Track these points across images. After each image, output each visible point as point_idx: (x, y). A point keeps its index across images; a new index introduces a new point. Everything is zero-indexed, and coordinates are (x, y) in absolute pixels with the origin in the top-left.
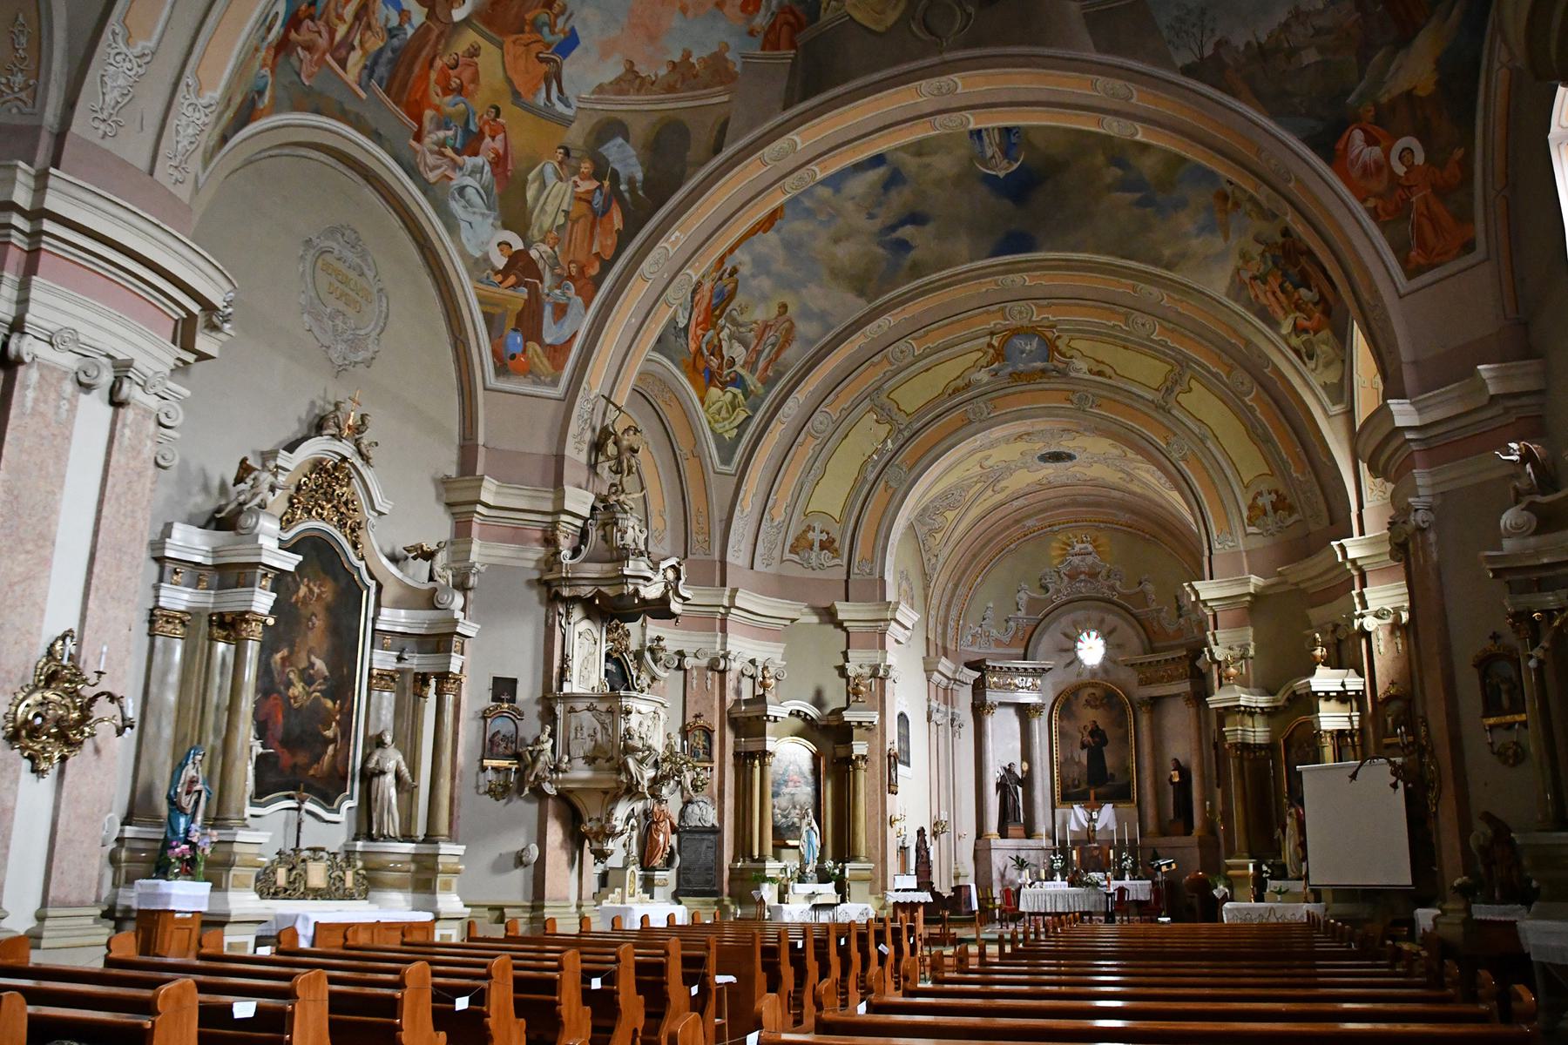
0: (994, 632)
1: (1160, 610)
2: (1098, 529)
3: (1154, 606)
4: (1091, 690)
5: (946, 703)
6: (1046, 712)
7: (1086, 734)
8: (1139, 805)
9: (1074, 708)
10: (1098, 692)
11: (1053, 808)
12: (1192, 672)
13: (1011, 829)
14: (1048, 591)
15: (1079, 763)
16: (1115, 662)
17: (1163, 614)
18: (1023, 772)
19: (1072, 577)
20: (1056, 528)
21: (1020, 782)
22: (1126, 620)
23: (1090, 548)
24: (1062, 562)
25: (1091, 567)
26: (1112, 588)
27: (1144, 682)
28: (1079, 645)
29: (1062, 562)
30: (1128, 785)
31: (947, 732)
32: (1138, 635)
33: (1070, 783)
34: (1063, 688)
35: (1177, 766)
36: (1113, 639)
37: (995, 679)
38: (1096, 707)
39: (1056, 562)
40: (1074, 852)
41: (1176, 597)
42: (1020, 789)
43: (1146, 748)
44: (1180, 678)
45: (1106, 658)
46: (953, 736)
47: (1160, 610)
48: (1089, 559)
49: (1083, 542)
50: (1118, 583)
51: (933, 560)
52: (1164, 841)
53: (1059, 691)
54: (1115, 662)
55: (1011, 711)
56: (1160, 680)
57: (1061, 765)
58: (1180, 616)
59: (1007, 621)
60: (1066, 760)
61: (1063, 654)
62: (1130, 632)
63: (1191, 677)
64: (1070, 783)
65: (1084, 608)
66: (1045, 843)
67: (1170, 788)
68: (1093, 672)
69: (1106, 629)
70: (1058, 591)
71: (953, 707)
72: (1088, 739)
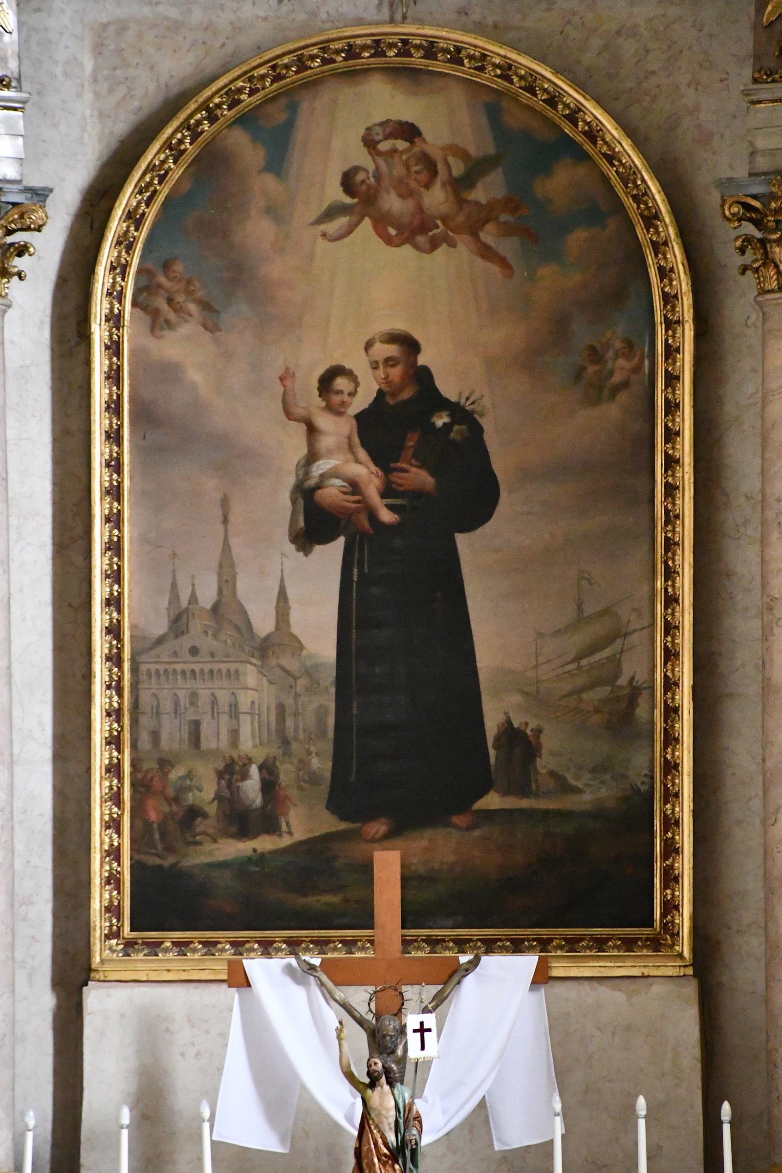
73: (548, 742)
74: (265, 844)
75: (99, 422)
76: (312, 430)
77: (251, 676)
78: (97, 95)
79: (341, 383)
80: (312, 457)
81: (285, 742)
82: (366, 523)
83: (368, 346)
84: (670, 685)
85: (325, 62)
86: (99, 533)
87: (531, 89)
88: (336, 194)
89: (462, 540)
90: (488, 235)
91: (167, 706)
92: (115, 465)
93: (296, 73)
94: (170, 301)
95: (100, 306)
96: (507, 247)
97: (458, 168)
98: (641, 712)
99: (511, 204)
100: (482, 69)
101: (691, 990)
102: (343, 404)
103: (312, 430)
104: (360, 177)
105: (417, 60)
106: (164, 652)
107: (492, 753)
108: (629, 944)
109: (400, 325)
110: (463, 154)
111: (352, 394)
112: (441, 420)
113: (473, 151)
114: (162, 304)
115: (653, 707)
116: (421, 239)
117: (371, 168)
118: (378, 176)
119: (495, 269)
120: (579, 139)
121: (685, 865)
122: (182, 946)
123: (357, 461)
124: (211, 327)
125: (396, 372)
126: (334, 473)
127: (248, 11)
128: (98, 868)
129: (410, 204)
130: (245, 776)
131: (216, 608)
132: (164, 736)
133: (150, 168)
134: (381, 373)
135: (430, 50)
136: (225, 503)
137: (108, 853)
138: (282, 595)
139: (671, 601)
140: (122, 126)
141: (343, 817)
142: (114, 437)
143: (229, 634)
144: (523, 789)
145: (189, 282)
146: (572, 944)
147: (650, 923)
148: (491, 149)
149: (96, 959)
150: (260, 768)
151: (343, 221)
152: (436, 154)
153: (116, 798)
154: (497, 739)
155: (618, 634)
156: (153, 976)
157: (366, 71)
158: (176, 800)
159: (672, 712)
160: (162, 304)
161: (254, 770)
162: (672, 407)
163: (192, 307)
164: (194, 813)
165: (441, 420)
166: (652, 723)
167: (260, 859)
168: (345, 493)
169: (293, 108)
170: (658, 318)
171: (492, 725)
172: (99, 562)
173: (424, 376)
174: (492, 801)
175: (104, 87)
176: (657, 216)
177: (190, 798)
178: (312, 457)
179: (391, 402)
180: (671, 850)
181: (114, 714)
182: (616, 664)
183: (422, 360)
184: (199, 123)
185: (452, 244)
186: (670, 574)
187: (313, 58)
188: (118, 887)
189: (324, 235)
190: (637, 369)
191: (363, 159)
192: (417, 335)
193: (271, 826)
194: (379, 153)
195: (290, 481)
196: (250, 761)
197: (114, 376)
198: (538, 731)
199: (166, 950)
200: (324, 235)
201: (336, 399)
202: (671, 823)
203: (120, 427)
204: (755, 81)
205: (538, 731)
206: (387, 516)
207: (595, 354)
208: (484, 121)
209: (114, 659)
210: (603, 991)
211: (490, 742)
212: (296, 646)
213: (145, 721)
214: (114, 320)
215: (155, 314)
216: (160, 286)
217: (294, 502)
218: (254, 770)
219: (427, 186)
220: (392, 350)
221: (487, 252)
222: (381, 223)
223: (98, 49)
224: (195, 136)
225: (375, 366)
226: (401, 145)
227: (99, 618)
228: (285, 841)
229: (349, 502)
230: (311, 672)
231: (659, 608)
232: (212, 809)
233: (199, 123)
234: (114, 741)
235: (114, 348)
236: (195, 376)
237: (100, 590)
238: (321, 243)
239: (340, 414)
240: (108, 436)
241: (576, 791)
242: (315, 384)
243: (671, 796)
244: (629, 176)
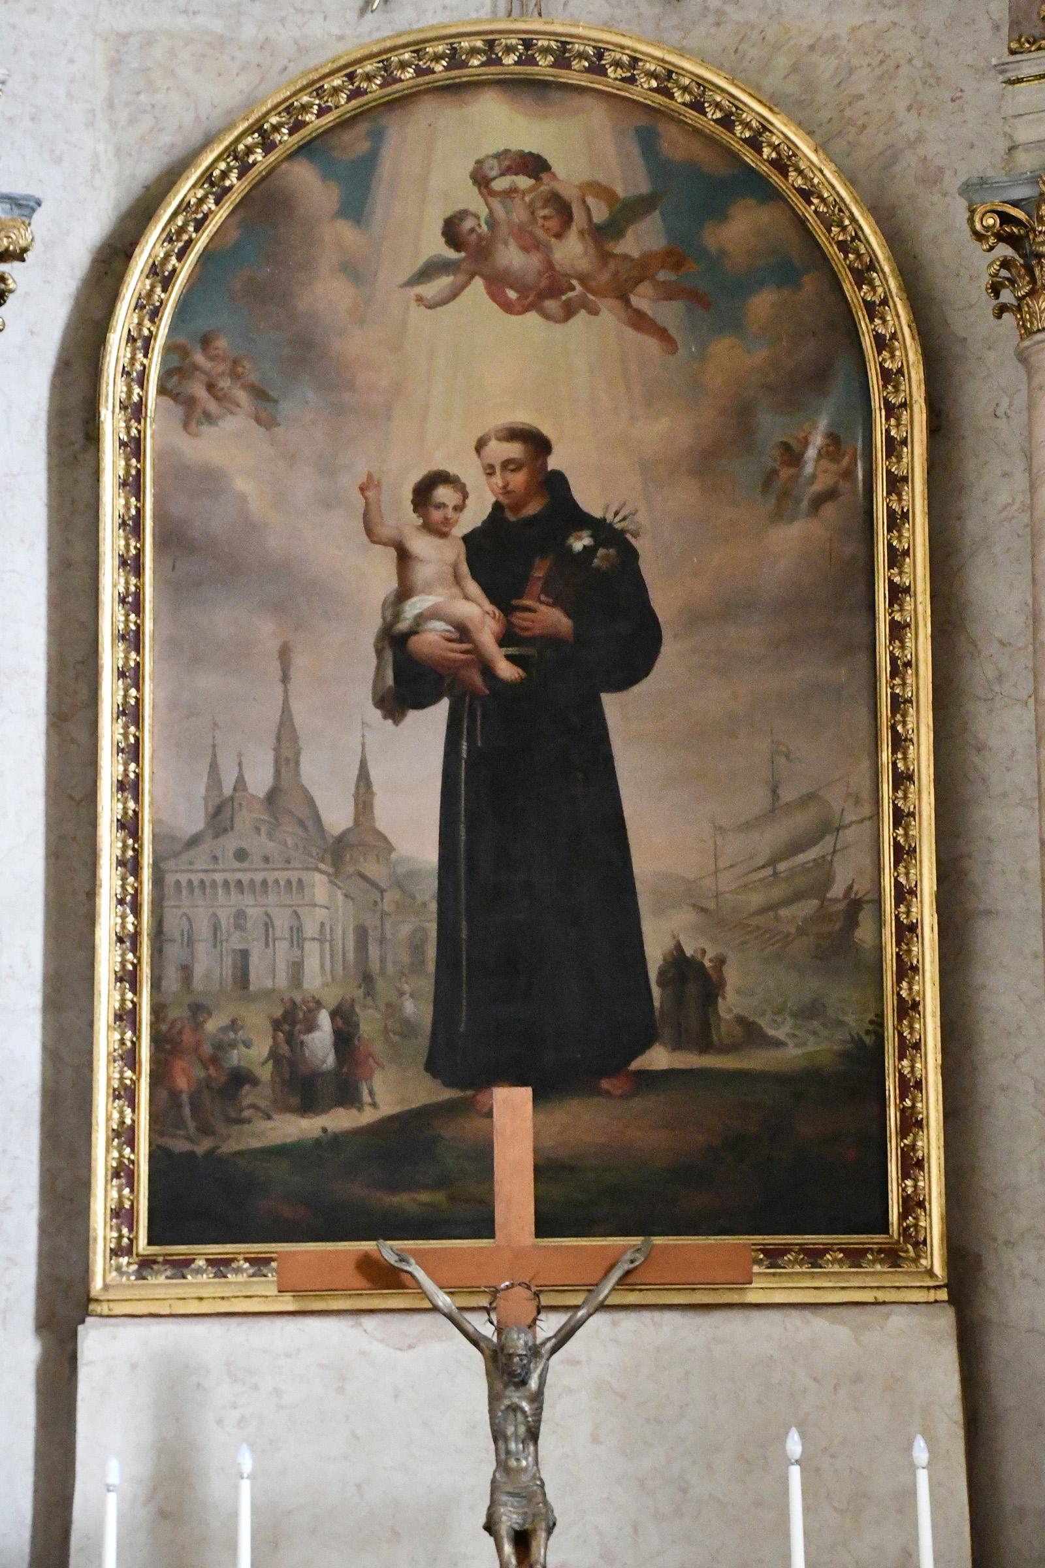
73: (732, 976)
74: (340, 1120)
75: (111, 543)
76: (404, 557)
77: (320, 886)
78: (113, 125)
79: (443, 494)
80: (404, 592)
81: (367, 979)
82: (477, 680)
83: (480, 445)
84: (904, 894)
85: (420, 72)
86: (110, 692)
87: (697, 106)
88: (436, 247)
89: (610, 702)
90: (642, 300)
91: (203, 930)
92: (133, 603)
93: (381, 86)
94: (211, 387)
95: (113, 388)
96: (669, 314)
97: (600, 212)
98: (863, 934)
99: (674, 258)
100: (632, 80)
101: (946, 1321)
102: (446, 521)
103: (404, 557)
104: (468, 224)
106: (200, 857)
107: (656, 991)
108: (855, 1256)
109: (523, 417)
110: (605, 193)
111: (459, 508)
112: (580, 542)
113: (620, 191)
114: (200, 392)
115: (880, 924)
116: (551, 305)
117: (484, 212)
118: (492, 222)
119: (651, 344)
120: (765, 168)
122: (220, 1265)
123: (467, 598)
124: (266, 421)
125: (518, 480)
126: (434, 614)
127: (317, 28)
128: (102, 1157)
130: (311, 1027)
131: (272, 797)
132: (199, 971)
133: (184, 207)
134: (498, 480)
136: (285, 654)
137: (117, 1134)
138: (364, 776)
140: (146, 168)
142: (132, 564)
143: (290, 833)
145: (235, 362)
146: (773, 1256)
147: (884, 1228)
148: (644, 188)
149: (97, 1284)
150: (333, 1015)
151: (444, 282)
152: (570, 193)
153: (130, 1058)
154: (662, 973)
155: (827, 827)
156: (181, 1308)
157: (475, 85)
158: (215, 1060)
159: (907, 931)
160: (200, 392)
161: (324, 1018)
163: (242, 396)
164: (240, 1078)
165: (580, 542)
166: (880, 948)
167: (333, 1142)
168: (449, 640)
169: (377, 137)
170: (876, 402)
171: (655, 952)
172: (109, 731)
173: (556, 485)
174: (658, 1058)
175: (123, 115)
176: (872, 266)
177: (235, 1057)
178: (404, 592)
179: (511, 517)
180: (911, 1123)
181: (128, 940)
182: (825, 867)
183: (553, 463)
184: (249, 150)
185: (594, 312)
186: (899, 743)
187: (403, 65)
188: (131, 1184)
189: (420, 299)
190: (849, 474)
191: (471, 200)
192: (547, 430)
193: (347, 1095)
194: (493, 193)
195: (374, 624)
196: (319, 1004)
197: (133, 485)
198: (720, 961)
199: (199, 1271)
200: (420, 299)
201: (436, 515)
202: (911, 1086)
203: (140, 552)
204: (1013, 52)
205: (720, 961)
206: (506, 670)
207: (792, 455)
208: (635, 150)
209: (130, 865)
210: (818, 1323)
211: (653, 975)
212: (384, 846)
213: (174, 952)
215: (189, 403)
216: (196, 367)
217: (379, 652)
218: (324, 1019)
219: (559, 236)
220: (514, 450)
221: (639, 321)
222: (497, 284)
223: (115, 64)
225: (490, 471)
226: (523, 182)
227: (109, 807)
228: (368, 1117)
229: (455, 652)
230: (403, 882)
231: (886, 789)
232: (265, 1073)
233: (249, 150)
234: (128, 978)
235: (133, 447)
236: (241, 484)
237: (109, 768)
238: (417, 314)
239: (443, 535)
240: (123, 563)
241: (779, 1044)
242: (409, 495)
243: (910, 1048)
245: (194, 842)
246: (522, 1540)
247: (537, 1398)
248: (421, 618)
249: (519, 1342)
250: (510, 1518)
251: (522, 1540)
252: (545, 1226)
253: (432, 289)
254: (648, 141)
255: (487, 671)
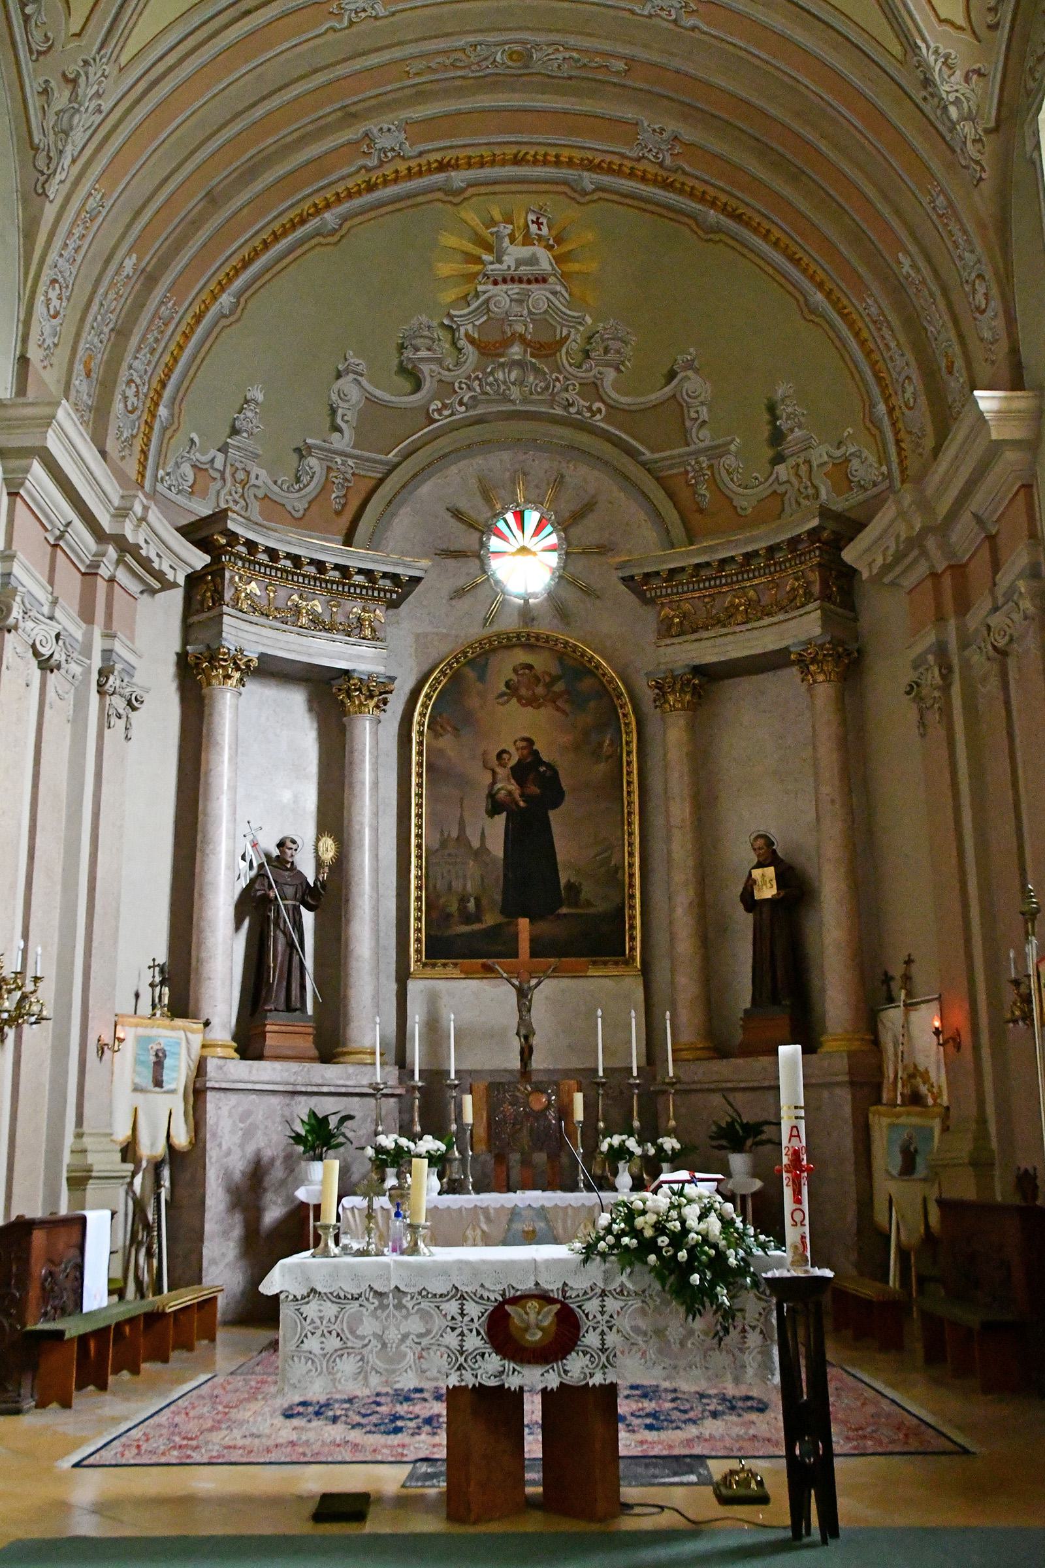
0: (261, 475)
1: (717, 452)
2: (576, 194)
3: (703, 438)
4: (521, 656)
5: (87, 615)
6: (396, 704)
7: (502, 772)
8: (646, 971)
9: (473, 702)
10: (541, 662)
11: (403, 976)
12: (825, 583)
13: (275, 1032)
14: (418, 387)
15: (481, 853)
16: (587, 592)
17: (730, 460)
18: (319, 864)
19: (490, 349)
20: (458, 178)
21: (311, 896)
22: (625, 478)
23: (545, 261)
24: (465, 300)
25: (541, 321)
26: (593, 389)
27: (667, 630)
28: (495, 543)
29: (465, 300)
30: (618, 916)
31: (80, 705)
32: (656, 515)
33: (454, 908)
34: (443, 648)
35: (768, 855)
36: (589, 531)
37: (253, 587)
38: (532, 702)
39: (450, 295)
40: (468, 1100)
41: (772, 409)
42: (308, 917)
43: (679, 810)
44: (790, 604)
45: (565, 577)
46: (105, 722)
47: (717, 452)
48: (539, 293)
49: (527, 240)
50: (611, 374)
51: (61, 99)
52: (723, 1069)
53: (434, 654)
54: (587, 592)
55: (295, 700)
56: (725, 619)
57: (431, 858)
58: (778, 459)
59: (301, 453)
60: (444, 844)
61: (451, 563)
62: (633, 511)
63: (826, 597)
64: (454, 908)
65: (518, 443)
66: (381, 1074)
67: (744, 921)
68: (526, 613)
69: (567, 506)
70: (446, 388)
71: (109, 635)
72: (507, 786)
74: (476, 927)
76: (494, 773)
77: (471, 863)
79: (505, 756)
80: (494, 783)
83: (515, 742)
84: (631, 865)
89: (552, 814)
92: (420, 785)
95: (415, 727)
96: (566, 707)
97: (547, 679)
98: (619, 875)
99: (567, 692)
101: (640, 980)
103: (494, 773)
105: (533, 640)
108: (616, 963)
109: (526, 735)
110: (550, 675)
112: (542, 769)
114: (439, 728)
121: (638, 933)
122: (444, 965)
125: (525, 752)
129: (530, 693)
130: (469, 901)
131: (457, 839)
135: (538, 638)
139: (631, 834)
140: (426, 668)
141: (507, 916)
142: (420, 775)
144: (576, 904)
146: (594, 963)
147: (624, 954)
148: (560, 673)
153: (419, 909)
154: (565, 887)
157: (514, 646)
159: (632, 876)
160: (439, 728)
161: (472, 900)
162: (629, 763)
164: (449, 916)
165: (542, 769)
167: (473, 934)
172: (414, 820)
173: (536, 753)
174: (564, 910)
176: (622, 694)
177: (448, 910)
178: (494, 783)
180: (632, 927)
181: (418, 878)
182: (609, 858)
186: (630, 824)
192: (534, 738)
197: (420, 753)
198: (580, 884)
202: (632, 917)
206: (522, 804)
207: (600, 745)
208: (557, 662)
209: (419, 857)
214: (421, 733)
220: (524, 744)
221: (558, 709)
222: (520, 699)
224: (451, 668)
225: (517, 749)
226: (527, 671)
228: (483, 926)
232: (456, 914)
234: (419, 888)
235: (420, 743)
243: (632, 907)
244: (612, 680)
245: (437, 850)
246: (526, 1038)
247: (530, 1001)
248: (499, 790)
249: (526, 986)
250: (523, 1032)
251: (526, 1038)
252: (534, 954)
253: (500, 700)
254: (561, 663)
255: (517, 804)
